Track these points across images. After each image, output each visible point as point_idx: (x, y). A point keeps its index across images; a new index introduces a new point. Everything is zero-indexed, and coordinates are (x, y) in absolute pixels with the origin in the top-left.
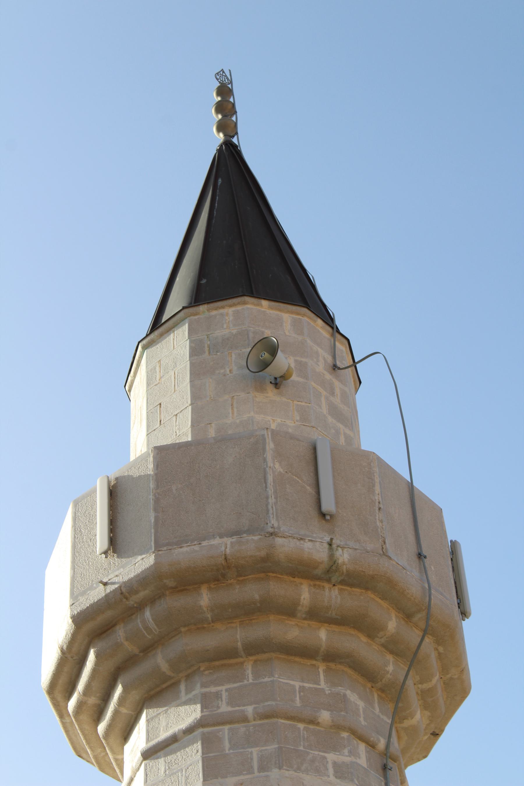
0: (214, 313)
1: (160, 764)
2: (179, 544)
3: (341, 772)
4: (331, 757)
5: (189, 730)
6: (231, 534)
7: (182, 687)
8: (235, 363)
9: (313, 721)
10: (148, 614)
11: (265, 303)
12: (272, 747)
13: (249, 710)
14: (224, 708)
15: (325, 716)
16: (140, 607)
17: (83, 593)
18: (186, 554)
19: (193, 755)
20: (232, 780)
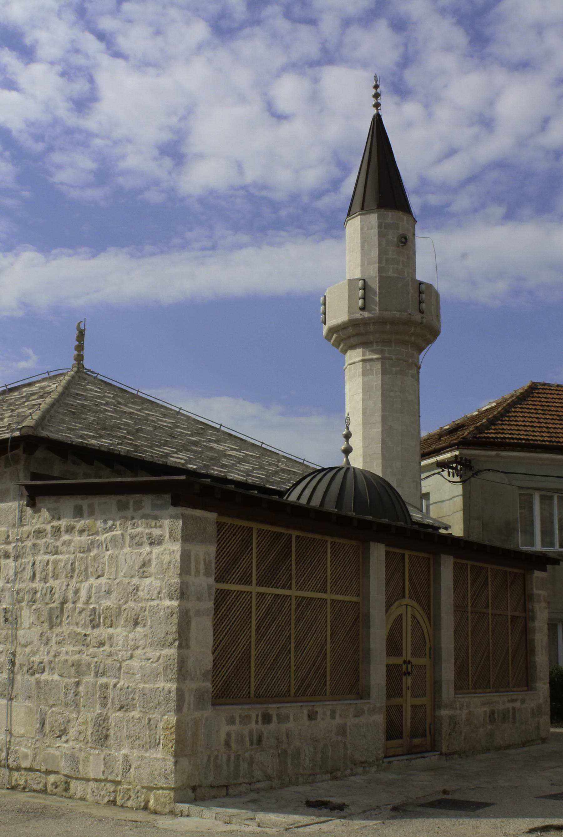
0: (385, 213)
1: (368, 366)
2: (386, 310)
3: (413, 376)
4: (411, 372)
5: (377, 359)
6: (399, 311)
7: (375, 344)
8: (392, 237)
9: (408, 362)
10: (371, 326)
11: (401, 212)
12: (398, 369)
13: (394, 357)
14: (387, 355)
15: (410, 360)
16: (369, 324)
17: (353, 314)
18: (387, 314)
19: (378, 366)
20: (388, 376)
